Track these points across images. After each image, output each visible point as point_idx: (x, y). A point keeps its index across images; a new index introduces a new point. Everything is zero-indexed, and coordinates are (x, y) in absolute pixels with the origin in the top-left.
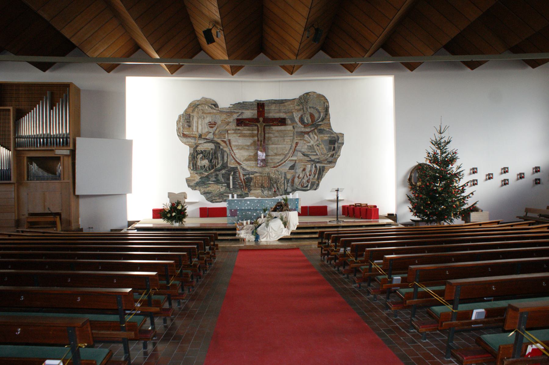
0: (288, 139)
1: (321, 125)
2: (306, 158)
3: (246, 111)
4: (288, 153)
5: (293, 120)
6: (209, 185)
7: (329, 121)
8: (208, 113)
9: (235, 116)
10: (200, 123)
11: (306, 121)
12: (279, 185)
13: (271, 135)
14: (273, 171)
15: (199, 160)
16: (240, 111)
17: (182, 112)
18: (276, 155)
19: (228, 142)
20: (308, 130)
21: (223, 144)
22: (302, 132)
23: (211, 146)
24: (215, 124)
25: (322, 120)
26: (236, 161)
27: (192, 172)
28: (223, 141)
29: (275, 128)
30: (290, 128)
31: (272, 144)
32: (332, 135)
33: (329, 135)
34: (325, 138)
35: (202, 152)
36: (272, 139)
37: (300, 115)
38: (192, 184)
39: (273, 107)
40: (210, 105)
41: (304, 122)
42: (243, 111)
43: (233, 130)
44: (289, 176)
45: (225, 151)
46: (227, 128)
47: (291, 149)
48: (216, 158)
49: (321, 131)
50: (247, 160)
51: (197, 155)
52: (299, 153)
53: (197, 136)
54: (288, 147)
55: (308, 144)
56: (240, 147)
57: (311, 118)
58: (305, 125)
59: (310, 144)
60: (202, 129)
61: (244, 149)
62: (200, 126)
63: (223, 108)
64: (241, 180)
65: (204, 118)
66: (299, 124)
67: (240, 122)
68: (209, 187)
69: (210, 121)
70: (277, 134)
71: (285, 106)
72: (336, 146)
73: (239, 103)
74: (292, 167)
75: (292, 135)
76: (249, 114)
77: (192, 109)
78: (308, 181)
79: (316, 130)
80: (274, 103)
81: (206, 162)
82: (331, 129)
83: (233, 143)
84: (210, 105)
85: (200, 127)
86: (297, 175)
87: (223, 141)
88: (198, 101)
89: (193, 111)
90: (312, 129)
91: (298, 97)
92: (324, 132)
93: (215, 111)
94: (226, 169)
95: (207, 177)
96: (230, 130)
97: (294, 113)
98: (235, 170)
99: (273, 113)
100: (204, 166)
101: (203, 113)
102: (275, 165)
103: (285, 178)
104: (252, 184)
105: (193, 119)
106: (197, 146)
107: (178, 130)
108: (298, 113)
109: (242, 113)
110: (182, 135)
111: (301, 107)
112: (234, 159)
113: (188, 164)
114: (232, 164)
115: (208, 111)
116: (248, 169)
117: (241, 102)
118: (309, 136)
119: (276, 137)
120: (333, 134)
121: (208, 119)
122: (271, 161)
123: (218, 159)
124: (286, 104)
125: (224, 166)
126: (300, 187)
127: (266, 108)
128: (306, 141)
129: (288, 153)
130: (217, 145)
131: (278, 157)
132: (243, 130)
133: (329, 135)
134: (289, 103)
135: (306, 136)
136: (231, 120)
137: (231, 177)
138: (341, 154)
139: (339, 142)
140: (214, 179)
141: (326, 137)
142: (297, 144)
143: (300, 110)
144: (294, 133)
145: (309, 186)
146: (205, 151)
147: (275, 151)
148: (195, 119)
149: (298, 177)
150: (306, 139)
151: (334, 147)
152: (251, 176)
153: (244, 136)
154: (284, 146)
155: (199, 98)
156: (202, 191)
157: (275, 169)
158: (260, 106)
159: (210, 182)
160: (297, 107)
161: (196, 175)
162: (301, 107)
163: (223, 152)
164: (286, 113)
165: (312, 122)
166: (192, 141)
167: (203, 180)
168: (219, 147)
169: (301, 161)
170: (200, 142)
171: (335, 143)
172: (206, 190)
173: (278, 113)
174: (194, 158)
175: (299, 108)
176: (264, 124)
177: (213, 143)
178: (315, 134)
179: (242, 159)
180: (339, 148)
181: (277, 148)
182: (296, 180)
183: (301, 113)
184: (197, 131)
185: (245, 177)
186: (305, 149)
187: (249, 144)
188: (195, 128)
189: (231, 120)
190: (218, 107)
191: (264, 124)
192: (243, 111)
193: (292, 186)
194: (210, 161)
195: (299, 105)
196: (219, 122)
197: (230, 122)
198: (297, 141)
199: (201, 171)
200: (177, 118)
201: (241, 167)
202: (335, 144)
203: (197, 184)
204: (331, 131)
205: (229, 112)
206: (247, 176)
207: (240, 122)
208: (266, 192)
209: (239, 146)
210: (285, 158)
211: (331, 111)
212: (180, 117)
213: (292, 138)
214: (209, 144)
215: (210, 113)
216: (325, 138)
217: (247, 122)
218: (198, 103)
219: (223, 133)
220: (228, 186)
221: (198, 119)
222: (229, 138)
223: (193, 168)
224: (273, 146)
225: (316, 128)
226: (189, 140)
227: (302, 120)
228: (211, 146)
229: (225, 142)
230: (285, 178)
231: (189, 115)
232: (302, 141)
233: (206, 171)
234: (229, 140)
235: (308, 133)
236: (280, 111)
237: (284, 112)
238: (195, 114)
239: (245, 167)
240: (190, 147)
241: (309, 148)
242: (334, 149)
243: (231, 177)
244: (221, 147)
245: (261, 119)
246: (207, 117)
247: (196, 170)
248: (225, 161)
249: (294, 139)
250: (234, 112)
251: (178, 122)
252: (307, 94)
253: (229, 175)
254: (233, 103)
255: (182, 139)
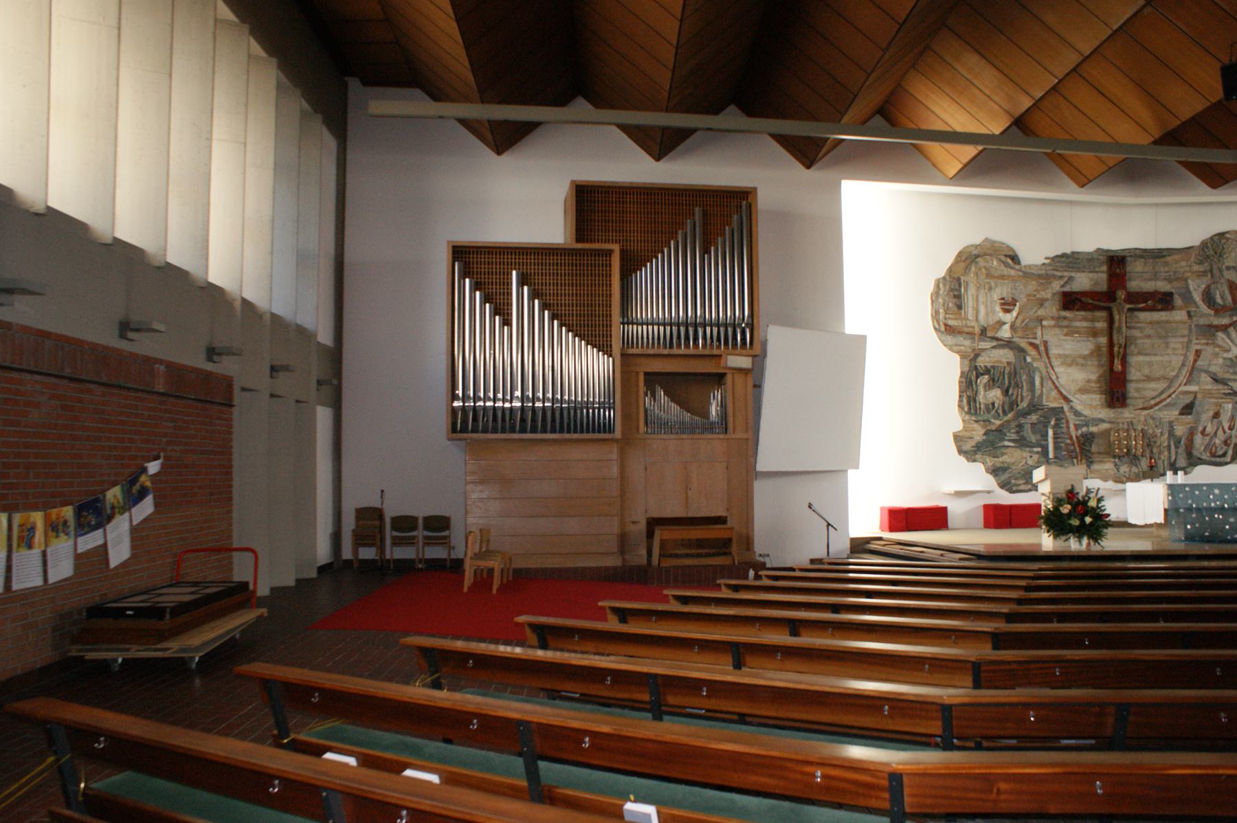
0: (1176, 343)
2: (1221, 387)
4: (1177, 377)
5: (1187, 297)
9: (1056, 286)
10: (981, 299)
11: (1219, 301)
12: (1155, 450)
13: (1136, 333)
14: (1142, 419)
16: (1066, 274)
18: (1149, 379)
19: (1042, 348)
21: (1033, 352)
22: (1211, 326)
26: (1061, 393)
27: (967, 417)
28: (1031, 344)
29: (1144, 316)
30: (1179, 315)
31: (1139, 354)
35: (987, 371)
36: (1139, 341)
37: (1203, 286)
38: (968, 446)
41: (1215, 302)
42: (1073, 274)
43: (1052, 318)
44: (1180, 430)
45: (1035, 369)
47: (1183, 365)
50: (1083, 391)
51: (977, 377)
52: (1203, 375)
53: (977, 330)
54: (1177, 361)
55: (1225, 355)
56: (1069, 360)
57: (1231, 293)
58: (1219, 310)
59: (1230, 355)
60: (987, 314)
61: (1077, 364)
64: (1071, 438)
65: (990, 289)
66: (1204, 308)
67: (1070, 301)
68: (1003, 454)
69: (1005, 295)
70: (1148, 331)
71: (1166, 264)
73: (1064, 255)
74: (1188, 409)
75: (1186, 332)
76: (1083, 282)
77: (962, 265)
78: (1226, 443)
80: (1141, 257)
81: (996, 395)
83: (1054, 351)
84: (1003, 258)
86: (1200, 429)
87: (1031, 344)
88: (977, 246)
89: (967, 270)
91: (1197, 243)
93: (1013, 272)
94: (1040, 413)
95: (999, 430)
97: (1190, 281)
98: (1058, 412)
102: (1146, 405)
103: (1171, 433)
104: (1094, 448)
105: (966, 290)
106: (977, 356)
108: (1197, 281)
109: (1071, 278)
110: (943, 329)
111: (1205, 267)
112: (1056, 387)
114: (1051, 401)
116: (1086, 412)
117: (1068, 252)
118: (1229, 336)
119: (1149, 337)
122: (1136, 395)
124: (1169, 259)
125: (1034, 407)
126: (1206, 456)
128: (1219, 346)
129: (1177, 377)
131: (1153, 385)
132: (1071, 320)
134: (1177, 257)
135: (1220, 335)
137: (1050, 432)
140: (1014, 436)
142: (1198, 353)
143: (1204, 274)
144: (1190, 330)
145: (1230, 452)
146: (993, 367)
147: (1146, 371)
148: (972, 291)
149: (1203, 432)
150: (1220, 342)
152: (1093, 429)
153: (1071, 332)
154: (1166, 358)
155: (978, 240)
156: (989, 464)
157: (1145, 412)
158: (1116, 262)
159: (1007, 443)
160: (1196, 268)
161: (976, 425)
162: (1205, 267)
164: (1170, 281)
167: (991, 438)
169: (1208, 394)
170: (983, 345)
173: (1150, 280)
175: (1201, 268)
176: (1128, 306)
177: (1011, 349)
179: (1073, 388)
181: (1150, 364)
182: (1198, 440)
184: (977, 320)
185: (1080, 432)
186: (1217, 367)
187: (1087, 353)
189: (1047, 294)
191: (1128, 306)
192: (1073, 274)
193: (1189, 454)
195: (1201, 263)
197: (1047, 300)
198: (1198, 347)
200: (931, 287)
201: (1071, 407)
205: (1042, 276)
206: (1084, 429)
207: (1070, 301)
208: (1124, 469)
209: (1066, 356)
210: (1169, 387)
213: (1186, 339)
215: (1002, 277)
218: (975, 252)
219: (1031, 325)
220: (1045, 452)
221: (978, 289)
222: (1045, 338)
224: (1141, 358)
226: (960, 339)
227: (1208, 298)
229: (1035, 346)
230: (1171, 433)
231: (959, 279)
232: (1210, 349)
233: (997, 416)
234: (1045, 343)
235: (1224, 328)
236: (1155, 277)
239: (1079, 408)
240: (963, 357)
241: (1228, 363)
243: (1050, 432)
245: (1121, 294)
246: (996, 285)
247: (976, 414)
248: (1038, 392)
249: (1190, 341)
250: (1054, 277)
251: (935, 295)
252: (1221, 235)
253: (1046, 427)
254: (1052, 255)
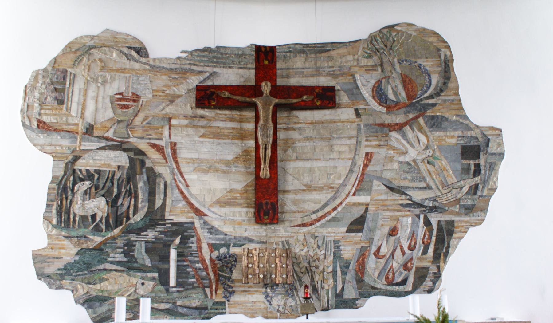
0: (342, 146)
1: (434, 105)
2: (397, 196)
3: (225, 71)
4: (344, 185)
5: (354, 92)
6: (104, 275)
7: (457, 94)
8: (117, 70)
9: (194, 81)
10: (91, 93)
11: (391, 96)
12: (317, 278)
13: (295, 135)
14: (301, 238)
15: (78, 198)
16: (208, 69)
17: (43, 63)
18: (309, 188)
19: (168, 151)
20: (399, 119)
21: (154, 155)
22: (382, 125)
23: (118, 160)
24: (136, 98)
25: (438, 93)
26: (191, 205)
27: (54, 232)
28: (154, 146)
29: (304, 115)
30: (346, 114)
31: (297, 158)
32: (469, 133)
33: (458, 133)
34: (450, 140)
35: (89, 176)
36: (298, 144)
37: (373, 82)
38: (52, 269)
39: (299, 62)
40: (126, 50)
41: (387, 99)
42: (216, 70)
43: (185, 117)
44: (349, 252)
45: (160, 175)
46: (168, 110)
47: (351, 171)
48: (133, 194)
49: (436, 123)
50: (221, 203)
51: (75, 183)
52: (375, 182)
53: (81, 128)
54: (343, 166)
55: (402, 159)
56: (204, 166)
57: (405, 87)
58: (392, 107)
59: (407, 158)
60: (96, 110)
61: (217, 170)
62: (91, 102)
63: (160, 60)
64: (203, 261)
65: (104, 82)
66: (374, 105)
67: (207, 97)
68: (102, 280)
69: (123, 89)
70: (309, 132)
71: (331, 58)
72: (482, 162)
73: (207, 50)
74: (357, 225)
75: (354, 133)
76: (230, 77)
77: (72, 56)
78: (406, 267)
79: (421, 120)
80: (303, 52)
81: (98, 206)
82: (466, 117)
83: (183, 154)
84: (126, 50)
85: (91, 106)
86: (374, 249)
87: (154, 146)
88: (93, 38)
89: (77, 62)
90: (411, 116)
91: (365, 36)
92: (445, 124)
93: (137, 66)
94: (160, 228)
95: (99, 249)
96: (176, 117)
97: (357, 76)
99: (297, 74)
100: (94, 216)
101: (103, 68)
102: (307, 220)
103: (337, 256)
104: (236, 275)
105: (72, 84)
106: (76, 158)
107: (26, 111)
108: (367, 76)
109: (213, 74)
110: (35, 123)
111: (375, 59)
112: (185, 197)
113: (44, 208)
114: (176, 213)
115: (118, 66)
116: (227, 229)
117: (213, 46)
118: (404, 136)
119: (309, 139)
120: (470, 129)
121: (117, 86)
122: (293, 208)
123: (136, 198)
124: (333, 53)
126: (381, 284)
127: (279, 65)
128: (394, 148)
129: (344, 185)
130: (137, 157)
131: (315, 196)
132: (214, 119)
133: (458, 133)
134: (342, 51)
135: (394, 134)
136: (182, 90)
137: (173, 253)
138: (499, 184)
139: (490, 150)
140: (121, 258)
141: (452, 138)
142: (369, 157)
143: (373, 68)
144: (359, 130)
145: (411, 280)
146: (99, 172)
147: (307, 179)
148: (79, 84)
149: (377, 254)
150: (394, 143)
151: (478, 166)
152: (234, 250)
153: (217, 135)
154: (331, 163)
155: (96, 31)
156: (81, 292)
157: (305, 229)
158: (265, 56)
159: (108, 266)
160: (364, 62)
161: (66, 242)
162: (375, 59)
163: (153, 177)
164: (334, 76)
165: (410, 97)
166: (64, 143)
167: (87, 258)
168: (143, 163)
169: (384, 206)
170: (86, 145)
171: (477, 154)
172: (95, 289)
173: (312, 76)
174: (65, 189)
175: (370, 62)
176: (277, 101)
177: (125, 150)
178: (421, 129)
179: (209, 199)
180: (493, 167)
181: (311, 170)
182: (372, 263)
183: (376, 75)
184: (82, 117)
185: (215, 254)
186: (392, 171)
187: (230, 157)
188: (75, 108)
189: (182, 90)
190: (147, 55)
191: (277, 101)
192: (216, 70)
193: (360, 281)
194: (113, 203)
195: (369, 57)
196: (146, 96)
197: (179, 96)
198: (369, 150)
199: (82, 231)
200: (26, 79)
201: (205, 223)
202: (479, 157)
203: (67, 271)
204: (463, 122)
205: (177, 70)
206: (223, 250)
207: (207, 97)
208: (278, 301)
209: (202, 161)
210: (334, 198)
211: (458, 68)
212: (36, 76)
213: (354, 141)
214: (112, 154)
215: (123, 70)
216: (450, 140)
217: (227, 94)
218: (92, 43)
219: (156, 124)
220: (164, 279)
221: (87, 82)
222: (173, 139)
223: (59, 221)
224: (300, 164)
225: (422, 115)
226: (56, 138)
227: (379, 93)
228: (118, 160)
229: (159, 149)
230: (337, 256)
231: (65, 72)
232: (383, 152)
233: (97, 230)
234: (173, 146)
235: (399, 128)
236: (318, 72)
237: (328, 75)
238: (80, 71)
239: (216, 224)
240: (56, 158)
241: (406, 168)
242: (477, 171)
243: (173, 253)
244: (148, 164)
245: (266, 87)
246: (113, 79)
247: (67, 226)
248: (158, 203)
249: (358, 143)
250: (192, 72)
251: (28, 90)
252: (391, 28)
253: (167, 246)
254: (190, 49)
255: (34, 135)
